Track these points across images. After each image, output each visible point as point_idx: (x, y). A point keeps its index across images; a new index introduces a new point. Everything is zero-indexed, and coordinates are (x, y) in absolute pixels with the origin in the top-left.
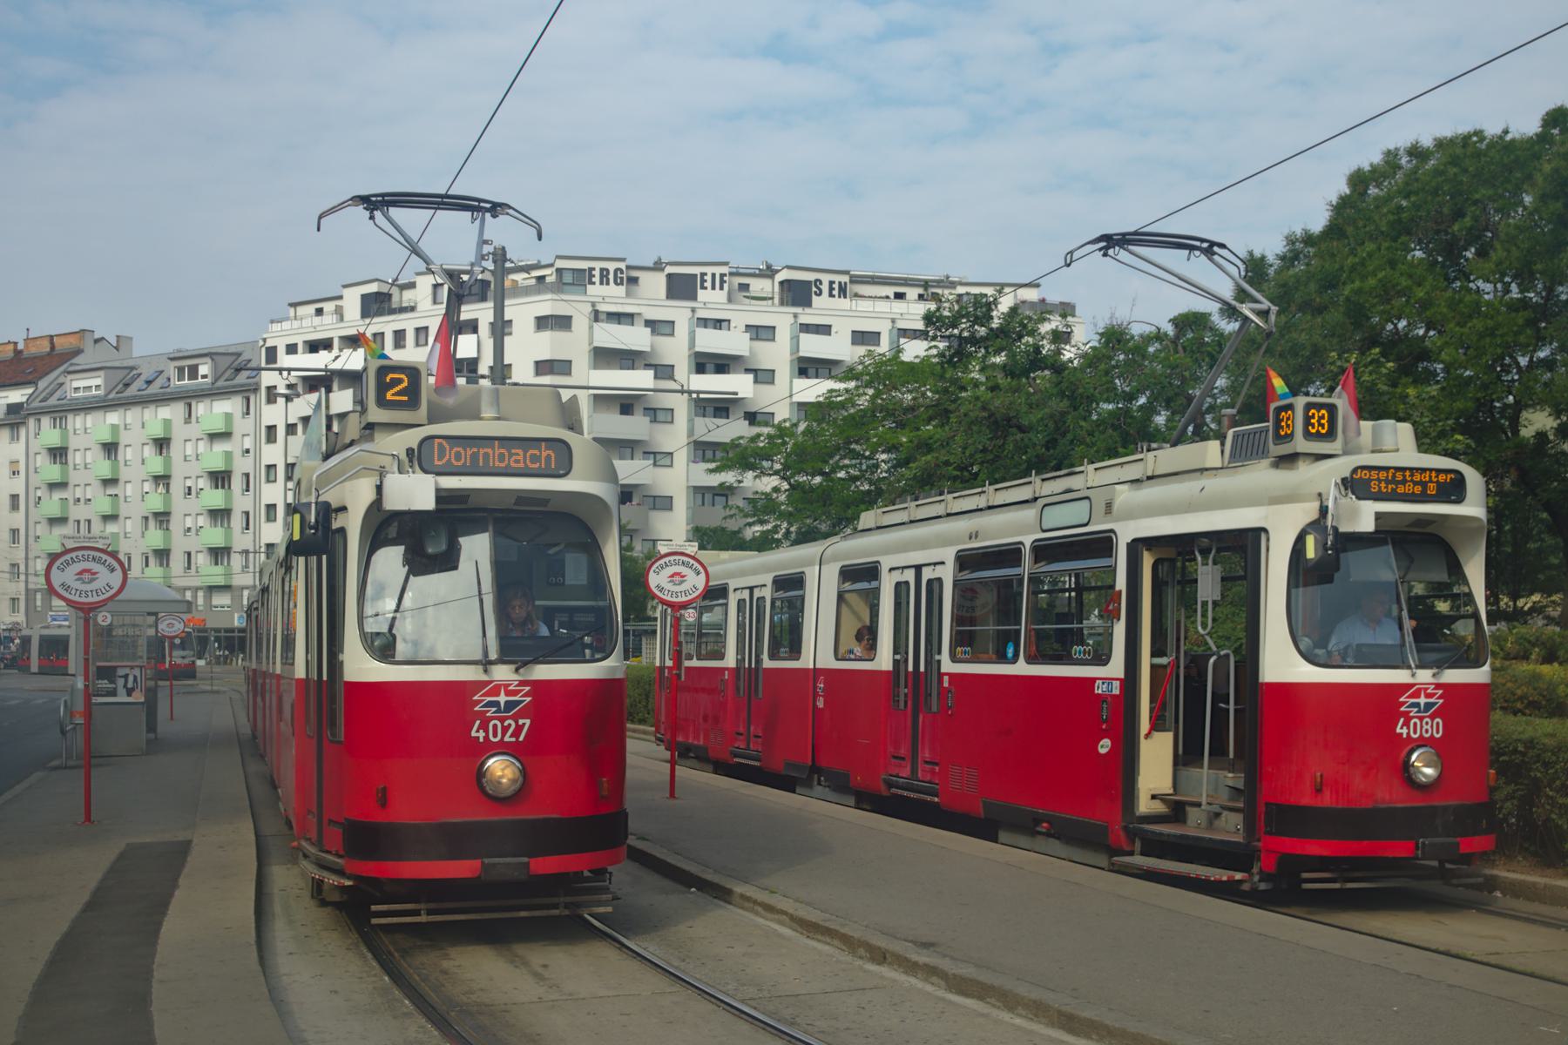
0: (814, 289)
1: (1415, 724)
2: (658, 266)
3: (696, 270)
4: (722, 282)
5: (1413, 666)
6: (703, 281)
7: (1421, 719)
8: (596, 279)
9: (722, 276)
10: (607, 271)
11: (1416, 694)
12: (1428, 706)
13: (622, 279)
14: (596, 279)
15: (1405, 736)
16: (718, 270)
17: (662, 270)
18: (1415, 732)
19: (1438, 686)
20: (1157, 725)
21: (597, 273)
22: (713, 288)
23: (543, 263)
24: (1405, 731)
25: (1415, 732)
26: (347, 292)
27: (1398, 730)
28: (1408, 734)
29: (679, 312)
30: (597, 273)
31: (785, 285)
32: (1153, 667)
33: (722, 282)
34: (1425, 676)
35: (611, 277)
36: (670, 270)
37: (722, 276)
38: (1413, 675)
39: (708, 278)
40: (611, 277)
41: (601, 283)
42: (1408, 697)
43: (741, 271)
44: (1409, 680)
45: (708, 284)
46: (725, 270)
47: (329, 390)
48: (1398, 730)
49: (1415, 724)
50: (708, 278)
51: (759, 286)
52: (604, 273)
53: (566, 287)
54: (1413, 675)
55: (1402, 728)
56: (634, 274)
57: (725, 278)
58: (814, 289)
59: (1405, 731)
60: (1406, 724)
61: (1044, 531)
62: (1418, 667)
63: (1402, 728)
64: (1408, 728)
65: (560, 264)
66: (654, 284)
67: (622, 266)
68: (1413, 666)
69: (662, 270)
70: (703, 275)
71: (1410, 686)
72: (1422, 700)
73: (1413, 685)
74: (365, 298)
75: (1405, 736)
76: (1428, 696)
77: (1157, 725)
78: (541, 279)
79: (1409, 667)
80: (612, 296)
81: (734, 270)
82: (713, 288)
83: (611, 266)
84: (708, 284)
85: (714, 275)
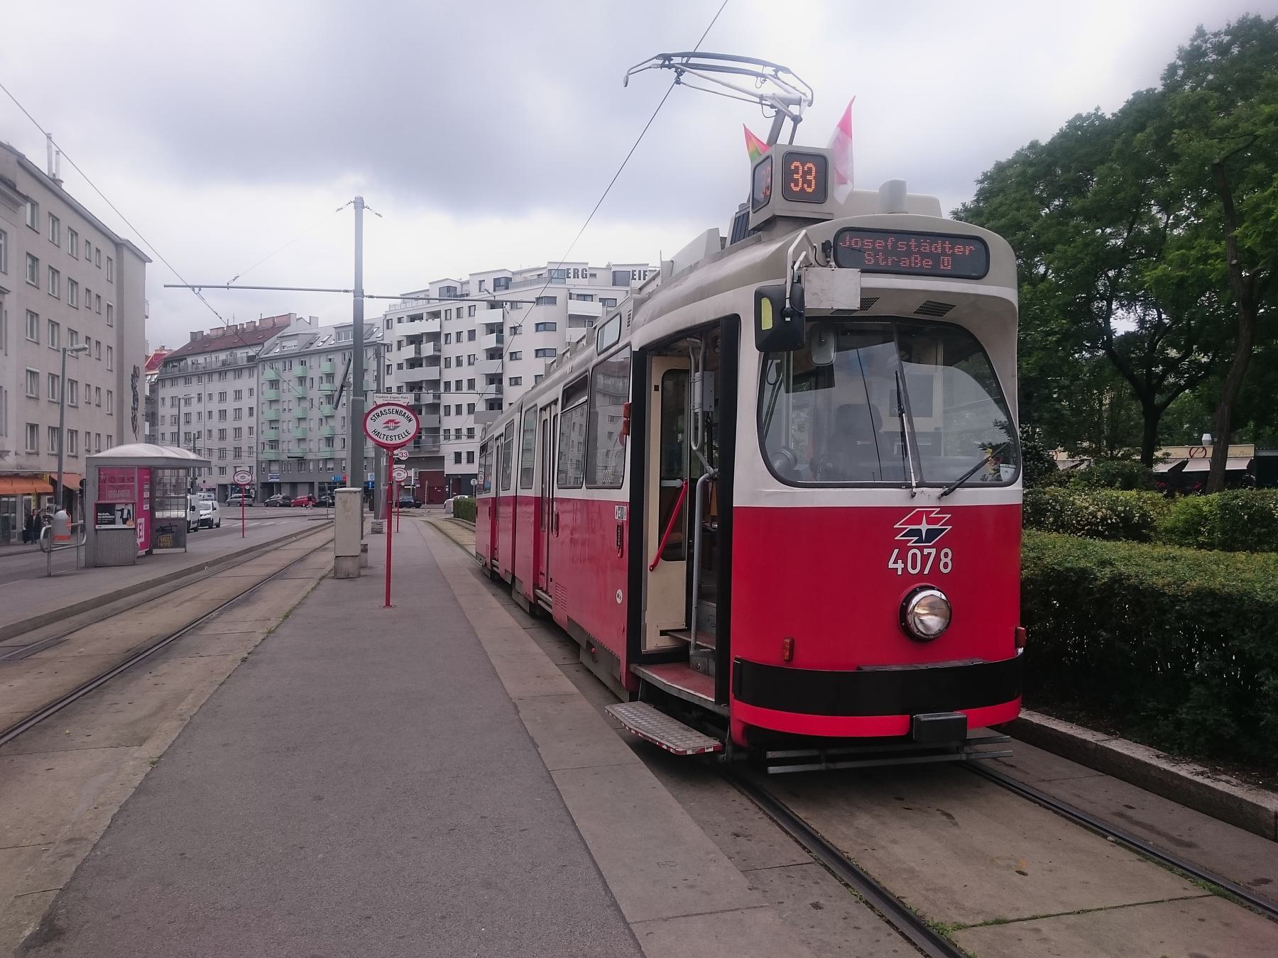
1: (914, 555)
7: (921, 549)
11: (917, 519)
12: (931, 534)
15: (900, 573)
18: (914, 567)
19: (944, 510)
25: (914, 567)
27: (891, 565)
28: (905, 569)
38: (913, 496)
42: (908, 522)
48: (891, 565)
49: (914, 555)
55: (896, 562)
59: (900, 566)
60: (902, 556)
63: (896, 562)
64: (905, 562)
68: (914, 484)
72: (924, 527)
75: (900, 573)
79: (909, 486)
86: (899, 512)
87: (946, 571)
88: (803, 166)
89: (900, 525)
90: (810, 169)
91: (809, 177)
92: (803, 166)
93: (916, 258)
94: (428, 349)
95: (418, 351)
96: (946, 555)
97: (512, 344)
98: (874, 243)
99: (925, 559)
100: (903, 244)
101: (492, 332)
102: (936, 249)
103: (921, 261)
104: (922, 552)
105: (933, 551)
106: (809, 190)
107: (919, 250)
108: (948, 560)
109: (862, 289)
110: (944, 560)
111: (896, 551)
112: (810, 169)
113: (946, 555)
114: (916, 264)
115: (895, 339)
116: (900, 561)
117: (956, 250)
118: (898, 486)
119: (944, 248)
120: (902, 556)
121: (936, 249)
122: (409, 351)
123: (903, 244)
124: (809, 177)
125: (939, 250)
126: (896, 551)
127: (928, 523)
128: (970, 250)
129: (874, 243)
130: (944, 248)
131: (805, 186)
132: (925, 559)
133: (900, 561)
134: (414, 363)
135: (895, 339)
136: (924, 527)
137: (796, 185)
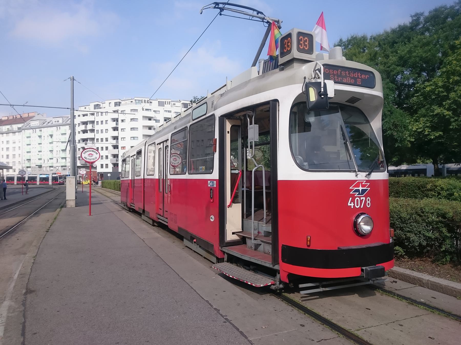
0: (189, 105)
1: (357, 200)
2: (156, 100)
3: (164, 101)
4: (170, 103)
5: (357, 171)
6: (166, 103)
7: (360, 197)
8: (143, 102)
9: (170, 102)
10: (145, 100)
11: (357, 185)
12: (363, 191)
13: (149, 102)
14: (143, 102)
15: (352, 207)
16: (169, 101)
17: (157, 100)
18: (357, 205)
19: (367, 181)
20: (234, 200)
21: (143, 101)
22: (168, 104)
23: (132, 99)
24: (352, 205)
25: (357, 205)
26: (91, 104)
27: (349, 204)
28: (354, 206)
29: (161, 109)
30: (143, 101)
31: (183, 104)
32: (232, 174)
33: (170, 103)
34: (362, 176)
35: (146, 102)
36: (159, 100)
37: (170, 102)
38: (356, 176)
39: (167, 102)
40: (146, 102)
41: (144, 103)
43: (173, 101)
44: (356, 179)
45: (167, 103)
46: (170, 101)
47: (87, 124)
48: (349, 204)
49: (357, 200)
50: (167, 102)
51: (178, 104)
52: (145, 101)
53: (137, 104)
54: (356, 176)
55: (351, 203)
56: (151, 101)
57: (170, 102)
58: (189, 105)
59: (352, 204)
60: (353, 201)
61: (193, 120)
62: (359, 171)
63: (351, 203)
64: (354, 203)
65: (135, 99)
66: (155, 103)
67: (149, 99)
68: (357, 171)
69: (157, 100)
70: (165, 102)
71: (355, 181)
72: (361, 188)
73: (357, 180)
74: (95, 105)
75: (352, 207)
76: (363, 186)
77: (234, 200)
78: (132, 102)
79: (355, 171)
80: (147, 106)
81: (172, 101)
82: (168, 104)
83: (146, 99)
84: (167, 103)
85: (168, 102)
86: (351, 182)
87: (369, 207)
88: (304, 38)
89: (352, 187)
90: (306, 40)
91: (306, 43)
92: (304, 38)
93: (349, 79)
94: (89, 127)
95: (86, 127)
96: (368, 200)
97: (121, 126)
98: (333, 72)
99: (361, 201)
100: (343, 74)
101: (114, 121)
102: (355, 76)
103: (350, 80)
104: (360, 199)
105: (364, 198)
106: (306, 49)
107: (349, 76)
108: (369, 202)
109: (335, 90)
110: (368, 202)
111: (351, 198)
112: (306, 40)
113: (368, 200)
114: (349, 81)
115: (340, 111)
116: (352, 203)
117: (362, 77)
118: (350, 171)
119: (358, 76)
120: (353, 201)
121: (355, 76)
122: (83, 127)
123: (343, 74)
124: (306, 43)
125: (357, 76)
126: (351, 198)
127: (362, 187)
128: (367, 77)
129: (333, 72)
130: (358, 76)
131: (305, 47)
132: (361, 201)
133: (352, 203)
134: (85, 131)
135: (340, 111)
136: (361, 188)
137: (302, 46)
